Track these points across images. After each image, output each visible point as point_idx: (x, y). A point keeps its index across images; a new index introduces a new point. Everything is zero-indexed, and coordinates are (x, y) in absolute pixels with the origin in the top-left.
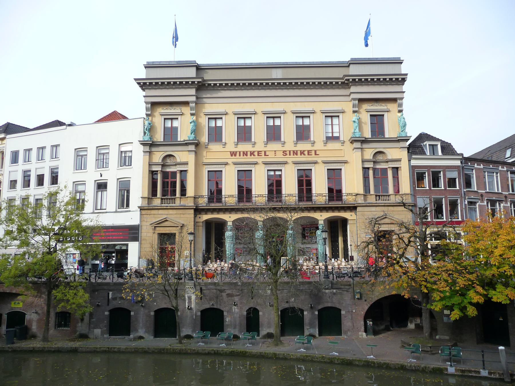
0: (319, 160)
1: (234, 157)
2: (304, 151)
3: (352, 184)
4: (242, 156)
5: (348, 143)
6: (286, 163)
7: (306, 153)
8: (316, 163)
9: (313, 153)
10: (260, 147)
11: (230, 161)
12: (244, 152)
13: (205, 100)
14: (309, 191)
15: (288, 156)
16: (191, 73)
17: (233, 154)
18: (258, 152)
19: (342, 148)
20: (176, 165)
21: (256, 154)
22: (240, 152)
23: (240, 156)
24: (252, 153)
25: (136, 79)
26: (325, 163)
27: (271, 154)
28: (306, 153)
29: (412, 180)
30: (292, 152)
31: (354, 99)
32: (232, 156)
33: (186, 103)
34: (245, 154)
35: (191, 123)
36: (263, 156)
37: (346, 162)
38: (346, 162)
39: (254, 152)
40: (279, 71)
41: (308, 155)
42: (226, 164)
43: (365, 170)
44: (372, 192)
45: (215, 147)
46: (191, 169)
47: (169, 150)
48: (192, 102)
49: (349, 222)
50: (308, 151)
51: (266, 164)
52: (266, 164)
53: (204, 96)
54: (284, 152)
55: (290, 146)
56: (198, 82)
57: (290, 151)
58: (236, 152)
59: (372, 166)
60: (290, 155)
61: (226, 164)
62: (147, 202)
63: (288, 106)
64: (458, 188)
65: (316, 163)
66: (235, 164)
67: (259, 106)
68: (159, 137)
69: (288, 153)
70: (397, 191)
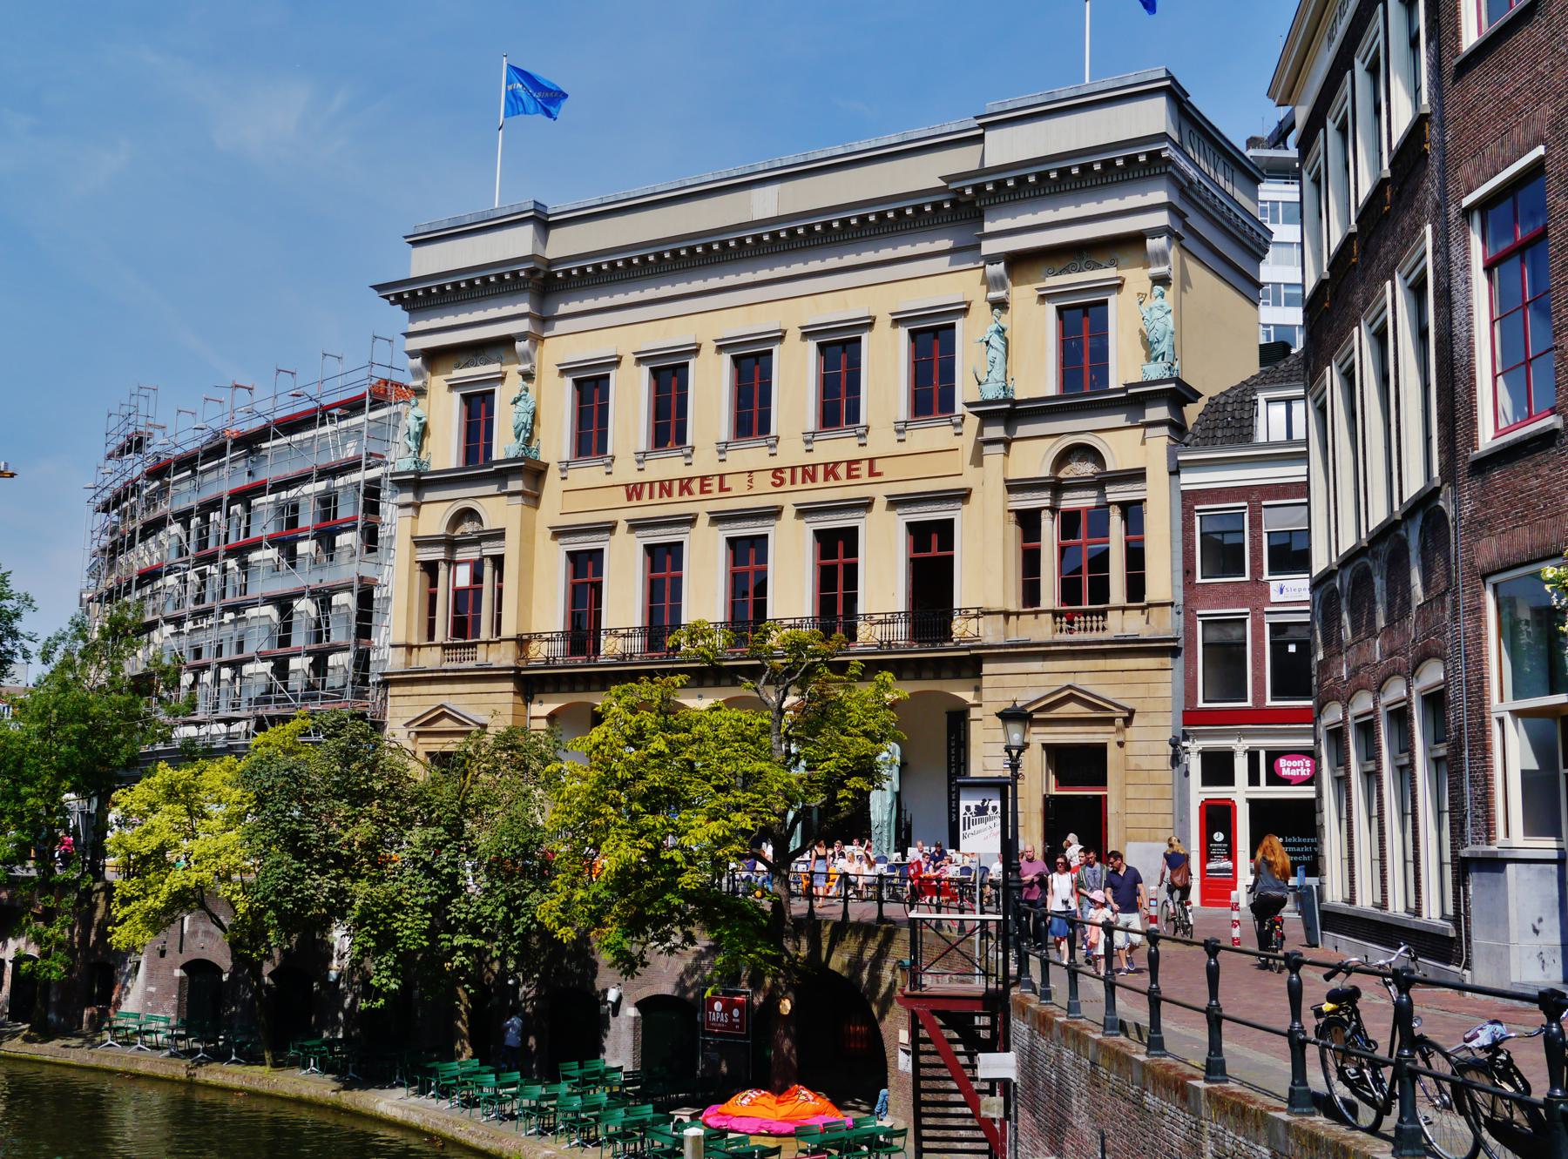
0: (880, 493)
1: (635, 502)
2: (836, 464)
3: (983, 574)
4: (656, 500)
5: (973, 422)
6: (775, 513)
7: (842, 470)
8: (866, 505)
9: (865, 466)
10: (705, 462)
11: (621, 517)
12: (661, 482)
13: (560, 326)
14: (761, 607)
15: (787, 486)
16: (518, 243)
17: (634, 491)
18: (703, 478)
19: (956, 442)
20: (477, 542)
21: (695, 486)
22: (651, 483)
23: (651, 497)
24: (685, 486)
25: (378, 288)
26: (895, 502)
27: (737, 484)
28: (842, 470)
29: (1179, 547)
30: (799, 472)
31: (992, 259)
32: (629, 498)
33: (507, 342)
34: (665, 488)
35: (515, 402)
36: (716, 494)
37: (963, 496)
38: (963, 496)
39: (690, 479)
40: (772, 190)
41: (849, 477)
42: (610, 528)
43: (1028, 522)
44: (1050, 595)
45: (589, 474)
46: (510, 549)
47: (463, 496)
48: (523, 336)
49: (974, 713)
50: (850, 463)
51: (718, 519)
52: (718, 519)
53: (563, 309)
54: (777, 471)
55: (791, 453)
56: (532, 272)
57: (793, 468)
58: (642, 484)
59: (1047, 503)
60: (793, 482)
61: (610, 528)
62: (403, 660)
63: (788, 309)
64: (1247, 578)
65: (866, 505)
66: (636, 526)
67: (704, 321)
68: (445, 452)
69: (787, 475)
70: (1136, 588)
